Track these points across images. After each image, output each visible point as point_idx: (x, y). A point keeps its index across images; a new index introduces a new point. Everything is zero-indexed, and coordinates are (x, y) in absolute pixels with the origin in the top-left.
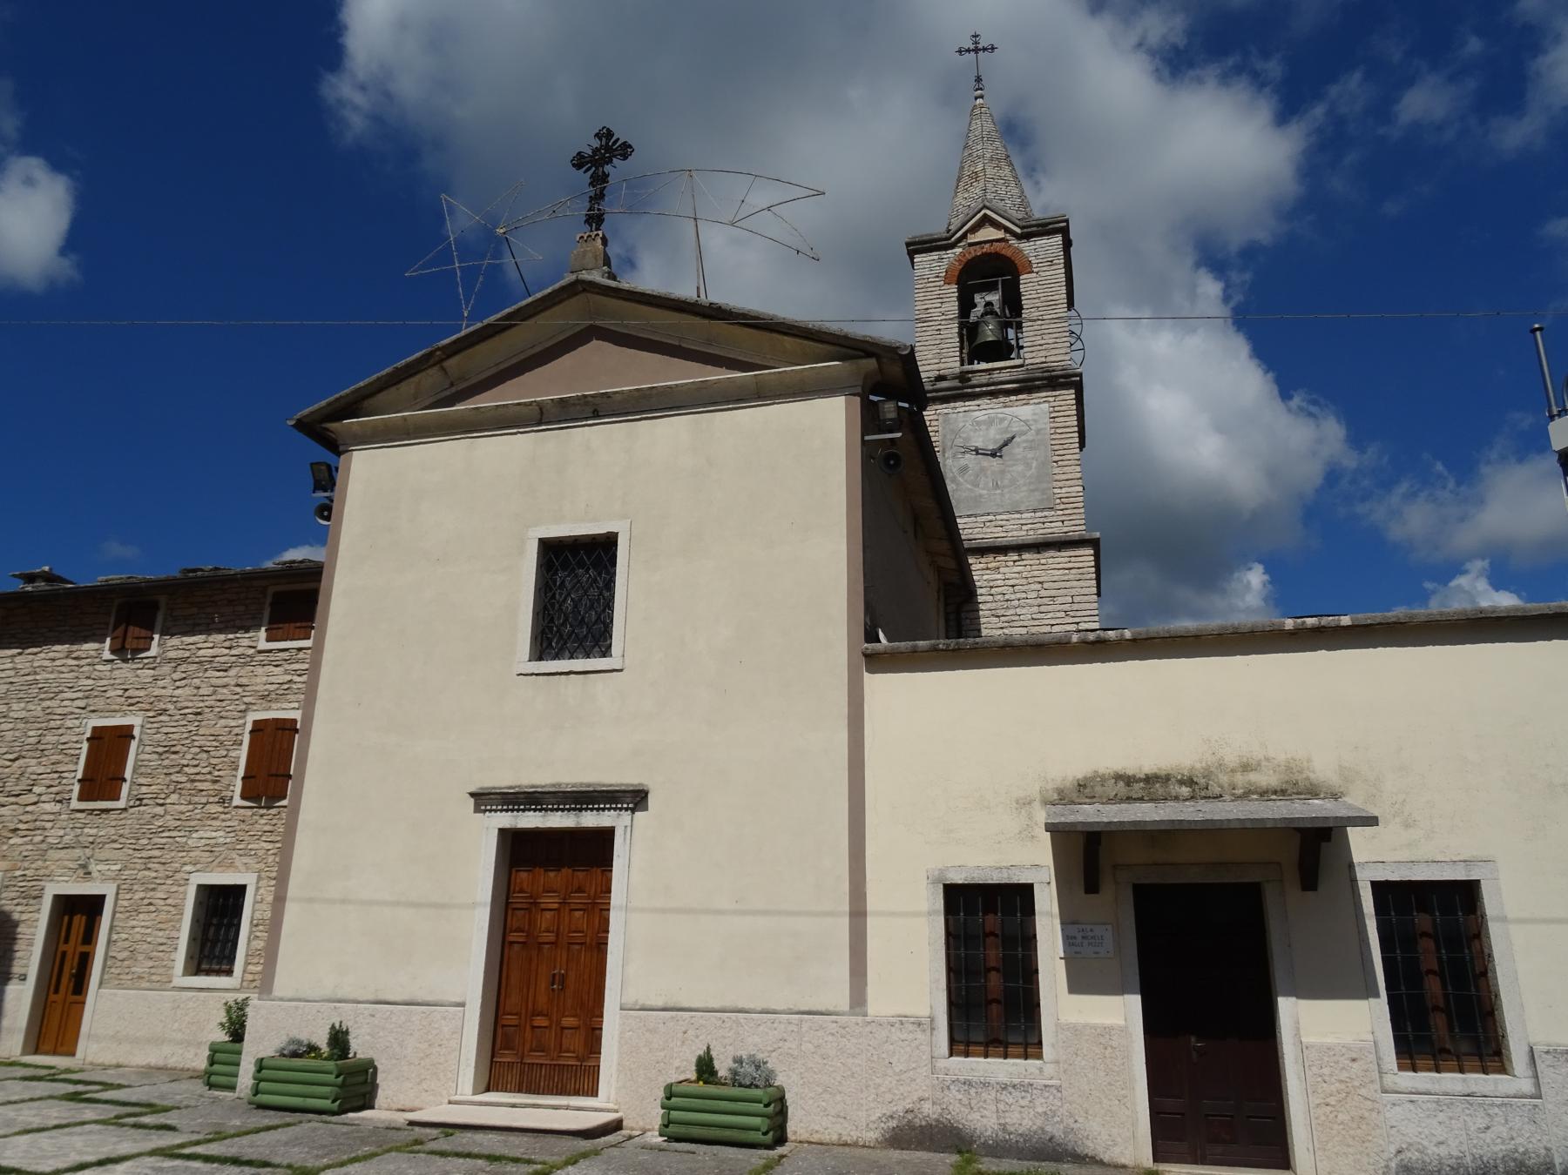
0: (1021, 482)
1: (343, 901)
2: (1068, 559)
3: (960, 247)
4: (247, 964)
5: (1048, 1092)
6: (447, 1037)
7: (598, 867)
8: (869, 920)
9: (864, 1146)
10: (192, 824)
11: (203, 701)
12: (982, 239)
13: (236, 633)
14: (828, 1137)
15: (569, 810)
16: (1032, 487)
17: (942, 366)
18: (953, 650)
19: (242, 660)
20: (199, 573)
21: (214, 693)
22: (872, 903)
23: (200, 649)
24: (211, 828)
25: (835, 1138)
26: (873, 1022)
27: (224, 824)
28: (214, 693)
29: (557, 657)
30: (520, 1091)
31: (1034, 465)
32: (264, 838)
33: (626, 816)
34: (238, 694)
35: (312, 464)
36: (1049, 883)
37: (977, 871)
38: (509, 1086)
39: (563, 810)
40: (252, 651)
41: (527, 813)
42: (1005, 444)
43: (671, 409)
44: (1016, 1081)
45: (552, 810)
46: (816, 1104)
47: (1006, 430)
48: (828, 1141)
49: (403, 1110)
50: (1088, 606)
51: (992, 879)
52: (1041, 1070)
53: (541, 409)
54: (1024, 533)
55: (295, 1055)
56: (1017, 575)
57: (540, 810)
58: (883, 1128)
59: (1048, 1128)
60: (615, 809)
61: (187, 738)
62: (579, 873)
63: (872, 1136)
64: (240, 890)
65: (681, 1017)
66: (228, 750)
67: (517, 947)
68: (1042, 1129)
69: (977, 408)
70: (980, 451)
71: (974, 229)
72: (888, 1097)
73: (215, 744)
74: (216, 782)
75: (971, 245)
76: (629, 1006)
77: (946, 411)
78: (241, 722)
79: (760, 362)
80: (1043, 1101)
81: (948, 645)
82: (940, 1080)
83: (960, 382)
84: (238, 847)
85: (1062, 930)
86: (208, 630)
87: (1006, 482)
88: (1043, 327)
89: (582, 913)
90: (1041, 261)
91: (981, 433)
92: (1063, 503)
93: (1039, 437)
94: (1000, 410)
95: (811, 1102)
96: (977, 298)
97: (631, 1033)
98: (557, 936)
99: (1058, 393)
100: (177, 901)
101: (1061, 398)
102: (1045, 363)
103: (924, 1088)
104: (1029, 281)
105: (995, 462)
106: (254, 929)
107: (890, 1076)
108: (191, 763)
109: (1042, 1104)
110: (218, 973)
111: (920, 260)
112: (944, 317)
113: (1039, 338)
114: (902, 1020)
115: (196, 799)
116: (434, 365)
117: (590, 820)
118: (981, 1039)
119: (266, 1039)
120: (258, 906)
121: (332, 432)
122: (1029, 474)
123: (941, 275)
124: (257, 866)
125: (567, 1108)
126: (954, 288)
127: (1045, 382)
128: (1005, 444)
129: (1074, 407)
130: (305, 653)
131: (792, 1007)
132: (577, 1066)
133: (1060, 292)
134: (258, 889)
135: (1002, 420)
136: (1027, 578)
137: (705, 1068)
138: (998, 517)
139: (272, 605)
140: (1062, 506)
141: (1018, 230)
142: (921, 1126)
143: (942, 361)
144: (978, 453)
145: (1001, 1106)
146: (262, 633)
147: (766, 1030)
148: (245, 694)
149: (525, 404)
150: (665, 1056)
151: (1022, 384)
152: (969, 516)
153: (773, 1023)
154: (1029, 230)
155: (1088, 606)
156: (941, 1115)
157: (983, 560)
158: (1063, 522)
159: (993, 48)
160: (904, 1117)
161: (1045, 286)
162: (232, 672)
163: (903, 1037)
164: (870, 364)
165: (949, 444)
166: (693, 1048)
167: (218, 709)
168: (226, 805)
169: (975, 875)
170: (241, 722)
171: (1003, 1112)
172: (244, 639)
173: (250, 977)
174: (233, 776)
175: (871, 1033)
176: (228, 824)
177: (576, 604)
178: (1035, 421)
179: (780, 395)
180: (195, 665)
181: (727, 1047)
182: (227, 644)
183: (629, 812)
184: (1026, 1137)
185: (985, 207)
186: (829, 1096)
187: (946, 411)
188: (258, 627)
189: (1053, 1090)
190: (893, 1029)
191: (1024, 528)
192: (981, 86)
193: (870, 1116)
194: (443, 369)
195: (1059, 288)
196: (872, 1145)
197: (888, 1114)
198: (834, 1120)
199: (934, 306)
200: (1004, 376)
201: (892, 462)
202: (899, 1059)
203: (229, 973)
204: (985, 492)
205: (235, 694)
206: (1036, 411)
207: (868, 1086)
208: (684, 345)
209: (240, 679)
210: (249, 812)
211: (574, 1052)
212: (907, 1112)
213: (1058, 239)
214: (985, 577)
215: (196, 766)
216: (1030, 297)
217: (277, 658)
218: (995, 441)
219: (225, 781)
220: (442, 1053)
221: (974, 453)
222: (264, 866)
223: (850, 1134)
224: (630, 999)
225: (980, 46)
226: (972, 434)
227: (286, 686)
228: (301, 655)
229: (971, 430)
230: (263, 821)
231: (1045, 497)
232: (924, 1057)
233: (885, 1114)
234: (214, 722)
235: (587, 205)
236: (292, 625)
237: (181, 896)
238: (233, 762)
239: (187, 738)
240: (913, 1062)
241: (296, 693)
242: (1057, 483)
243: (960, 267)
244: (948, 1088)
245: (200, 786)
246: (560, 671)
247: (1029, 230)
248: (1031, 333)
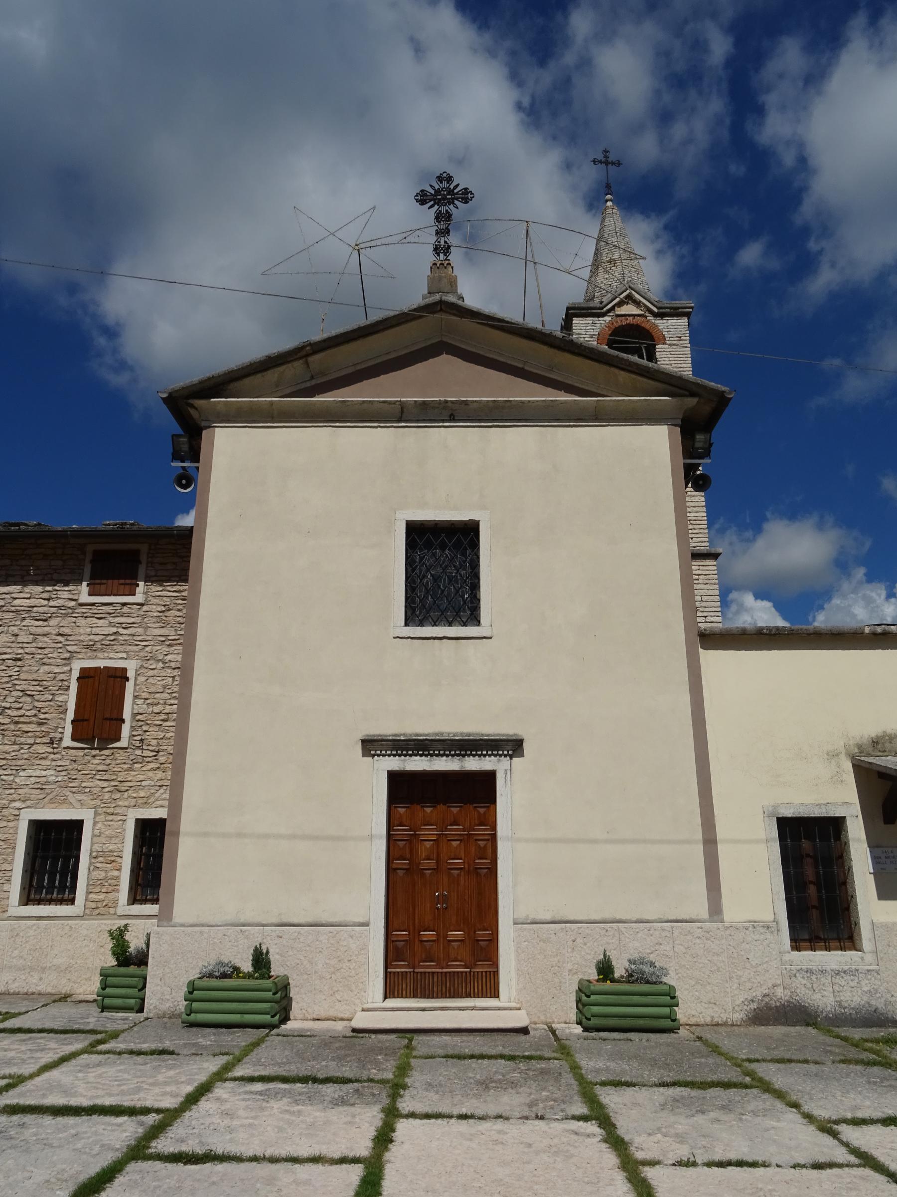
1: (240, 835)
3: (609, 316)
4: (89, 892)
5: (870, 975)
6: (357, 953)
7: (470, 804)
8: (720, 846)
9: (733, 1025)
10: (19, 763)
11: (22, 648)
12: (627, 313)
13: (55, 585)
14: (702, 1019)
15: (453, 756)
18: (775, 635)
19: (63, 612)
20: (23, 528)
21: (35, 640)
22: (722, 831)
23: (15, 599)
24: (40, 767)
25: (708, 1020)
26: (731, 927)
27: (54, 763)
28: (35, 640)
29: (421, 624)
30: (415, 996)
32: (98, 777)
33: (505, 761)
34: (61, 642)
35: (173, 436)
36: (857, 816)
37: (801, 808)
38: (404, 993)
39: (447, 756)
40: (73, 603)
41: (414, 758)
43: (519, 420)
44: (846, 968)
45: (437, 755)
46: (691, 994)
48: (703, 1023)
49: (318, 1020)
50: (712, 604)
51: (814, 814)
52: (862, 959)
53: (402, 408)
55: (224, 976)
57: (426, 756)
58: (746, 1010)
59: (873, 1002)
60: (495, 755)
61: (7, 682)
62: (399, 809)
63: (738, 1016)
64: (78, 825)
65: (570, 928)
66: (53, 695)
67: (400, 873)
68: (869, 1003)
72: (748, 985)
73: (38, 688)
74: (42, 724)
75: (618, 316)
76: (521, 921)
78: (66, 669)
79: (595, 391)
80: (867, 982)
82: (788, 970)
84: (71, 785)
85: (871, 852)
86: (24, 581)
89: (459, 842)
90: (672, 336)
95: (686, 992)
97: (526, 943)
98: (438, 863)
100: (7, 836)
103: (777, 977)
104: (663, 350)
106: (93, 861)
107: (749, 969)
108: (13, 705)
109: (866, 984)
110: (61, 902)
111: (578, 322)
114: (753, 924)
115: (22, 740)
116: (300, 358)
117: (473, 764)
118: (807, 937)
119: (172, 962)
120: (96, 839)
121: (196, 409)
124: (93, 802)
125: (474, 1008)
130: (130, 608)
131: (662, 917)
132: (466, 972)
133: (687, 362)
134: (95, 823)
137: (605, 969)
139: (92, 561)
141: (656, 310)
142: (776, 1007)
145: (836, 988)
146: (84, 588)
147: (644, 936)
148: (68, 643)
149: (390, 403)
150: (559, 962)
153: (649, 930)
154: (664, 310)
155: (712, 604)
156: (791, 997)
160: (762, 1001)
161: (676, 356)
162: (53, 622)
163: (756, 938)
164: (692, 402)
166: (583, 953)
167: (41, 656)
168: (55, 746)
169: (801, 810)
170: (66, 669)
171: (838, 992)
172: (64, 593)
173: (94, 905)
174: (61, 719)
175: (730, 935)
176: (59, 763)
177: (436, 579)
179: (614, 419)
180: (11, 614)
181: (612, 951)
182: (46, 595)
183: (508, 757)
184: (857, 1010)
186: (700, 987)
188: (80, 582)
189: (873, 973)
190: (747, 932)
192: (610, 192)
193: (735, 1001)
194: (307, 363)
195: (686, 359)
196: (739, 1023)
197: (749, 998)
198: (706, 1006)
201: (701, 482)
202: (754, 955)
203: (72, 901)
205: (57, 643)
207: (731, 978)
208: (526, 368)
209: (62, 629)
210: (81, 753)
211: (461, 961)
212: (764, 996)
215: (20, 709)
217: (101, 611)
219: (52, 724)
220: (352, 968)
222: (100, 802)
223: (723, 1017)
224: (521, 915)
225: (610, 160)
227: (112, 638)
228: (125, 609)
230: (96, 761)
232: (774, 953)
233: (746, 999)
234: (36, 668)
235: (433, 239)
236: (116, 581)
237: (11, 831)
238: (61, 706)
239: (7, 682)
240: (766, 957)
241: (123, 645)
244: (795, 976)
245: (25, 727)
246: (434, 636)
247: (664, 310)
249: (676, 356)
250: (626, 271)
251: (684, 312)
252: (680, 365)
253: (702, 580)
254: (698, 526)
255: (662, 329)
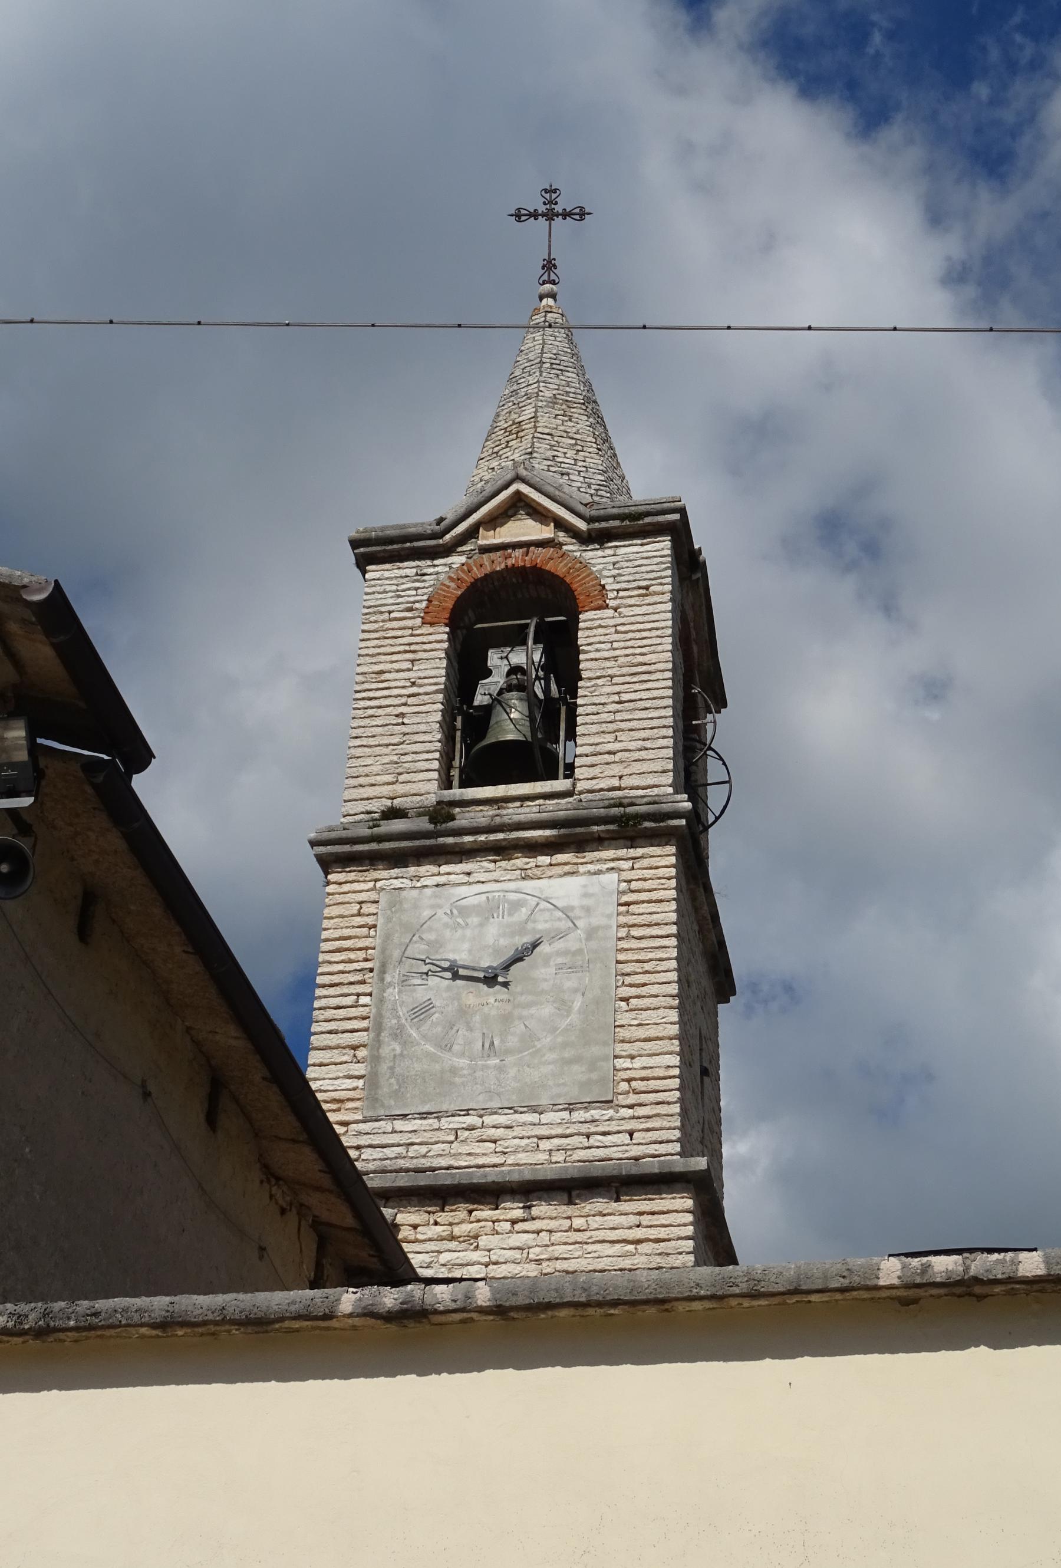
0: (547, 1040)
2: (633, 1219)
3: (463, 553)
16: (568, 1054)
17: (400, 789)
31: (577, 1005)
42: (518, 959)
47: (522, 929)
54: (542, 1157)
56: (517, 1255)
69: (466, 879)
70: (462, 972)
71: (494, 521)
75: (485, 550)
77: (397, 883)
81: (21, 1317)
83: (431, 822)
87: (513, 1041)
88: (619, 717)
91: (468, 933)
92: (636, 1092)
93: (593, 944)
94: (512, 886)
96: (494, 658)
99: (639, 852)
101: (645, 862)
102: (619, 789)
104: (597, 623)
105: (493, 996)
111: (377, 575)
112: (415, 690)
113: (610, 737)
122: (563, 1024)
123: (417, 605)
126: (441, 633)
127: (611, 827)
128: (518, 959)
129: (673, 883)
133: (660, 648)
135: (516, 906)
136: (539, 1262)
138: (489, 1120)
140: (632, 1099)
141: (582, 525)
143: (401, 778)
144: (456, 976)
151: (563, 831)
152: (424, 1116)
154: (604, 525)
157: (443, 1217)
158: (631, 1135)
159: (582, 214)
161: (630, 635)
165: (396, 954)
178: (588, 910)
185: (518, 478)
187: (397, 883)
191: (545, 1145)
192: (553, 276)
195: (659, 641)
199: (396, 666)
200: (530, 812)
204: (463, 1062)
206: (591, 890)
213: (663, 546)
214: (444, 1258)
216: (597, 655)
218: (497, 951)
221: (448, 975)
225: (558, 209)
226: (448, 933)
229: (446, 925)
231: (594, 1076)
242: (626, 1046)
243: (460, 593)
247: (604, 525)
248: (594, 729)
249: (630, 635)
250: (542, 447)
251: (658, 523)
252: (640, 659)
253: (644, 1259)
254: (652, 1097)
255: (600, 571)
